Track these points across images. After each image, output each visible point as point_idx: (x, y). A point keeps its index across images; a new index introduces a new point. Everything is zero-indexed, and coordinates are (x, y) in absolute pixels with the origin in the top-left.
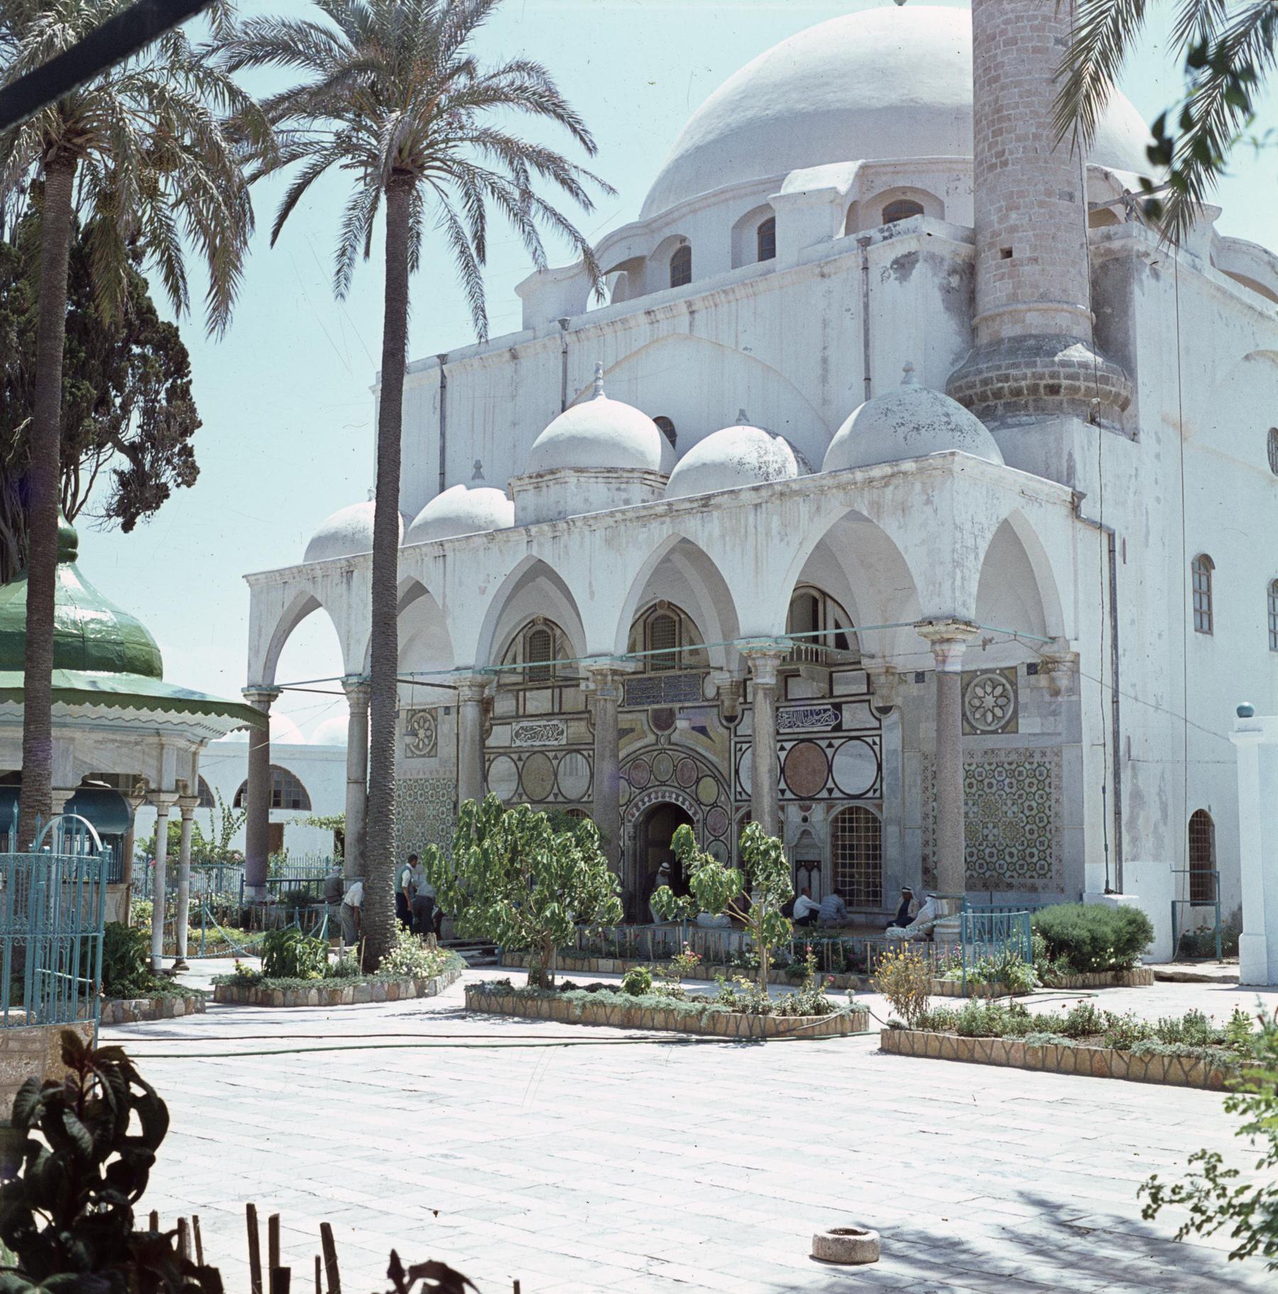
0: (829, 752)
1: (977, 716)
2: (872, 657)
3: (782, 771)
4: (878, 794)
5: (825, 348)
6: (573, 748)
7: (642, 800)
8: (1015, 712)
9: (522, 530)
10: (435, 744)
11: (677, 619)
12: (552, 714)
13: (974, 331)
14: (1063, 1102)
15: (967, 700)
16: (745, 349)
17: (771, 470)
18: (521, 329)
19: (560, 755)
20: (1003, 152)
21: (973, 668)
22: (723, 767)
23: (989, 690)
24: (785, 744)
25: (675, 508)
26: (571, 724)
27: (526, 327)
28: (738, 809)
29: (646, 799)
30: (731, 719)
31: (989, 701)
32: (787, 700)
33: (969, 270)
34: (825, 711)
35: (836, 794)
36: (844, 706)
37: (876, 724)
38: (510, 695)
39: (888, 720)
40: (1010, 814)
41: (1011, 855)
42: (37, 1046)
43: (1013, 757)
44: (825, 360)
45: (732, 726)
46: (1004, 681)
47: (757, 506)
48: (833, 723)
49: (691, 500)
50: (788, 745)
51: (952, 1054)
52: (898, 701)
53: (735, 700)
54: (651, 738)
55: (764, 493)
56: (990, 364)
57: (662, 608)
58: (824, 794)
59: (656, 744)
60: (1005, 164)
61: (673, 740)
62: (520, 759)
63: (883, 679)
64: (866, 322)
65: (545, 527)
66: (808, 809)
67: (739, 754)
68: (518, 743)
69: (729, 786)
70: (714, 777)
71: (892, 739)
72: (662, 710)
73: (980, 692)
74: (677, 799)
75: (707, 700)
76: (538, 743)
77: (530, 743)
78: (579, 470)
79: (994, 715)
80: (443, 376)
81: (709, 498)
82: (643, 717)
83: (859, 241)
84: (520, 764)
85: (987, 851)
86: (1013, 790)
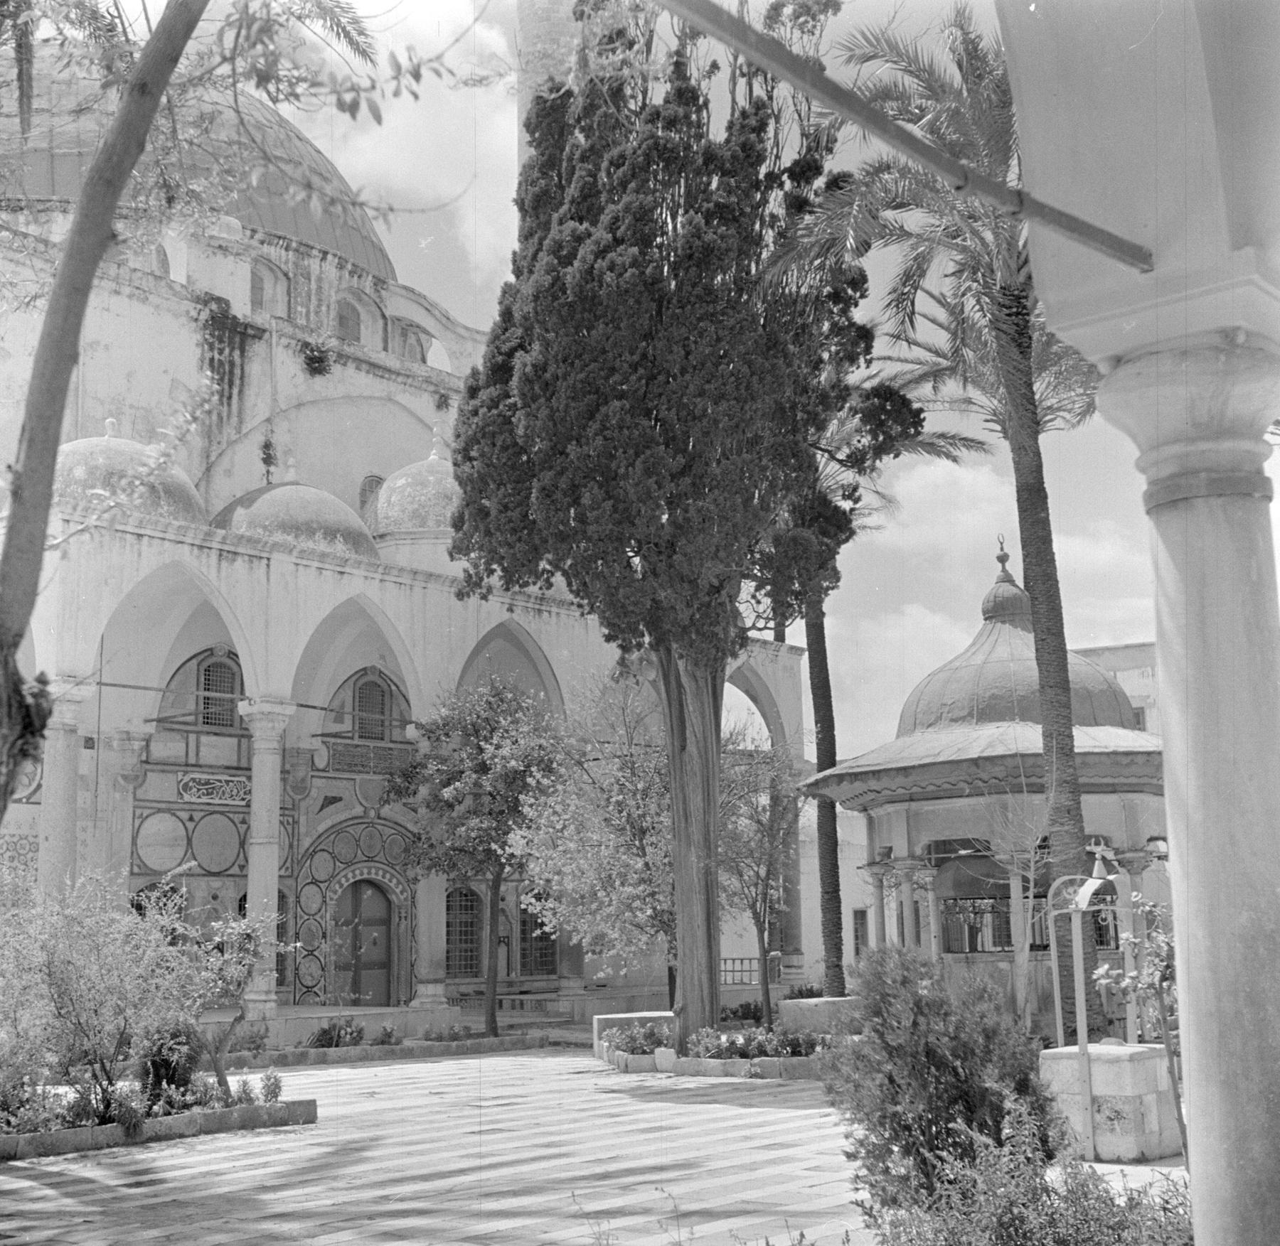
7: (345, 876)
10: (39, 786)
11: (386, 687)
29: (350, 875)
38: (178, 737)
57: (373, 673)
61: (383, 815)
62: (191, 819)
68: (187, 797)
74: (384, 877)
75: (318, 770)
76: (217, 801)
77: (205, 799)
82: (349, 784)
84: (190, 825)
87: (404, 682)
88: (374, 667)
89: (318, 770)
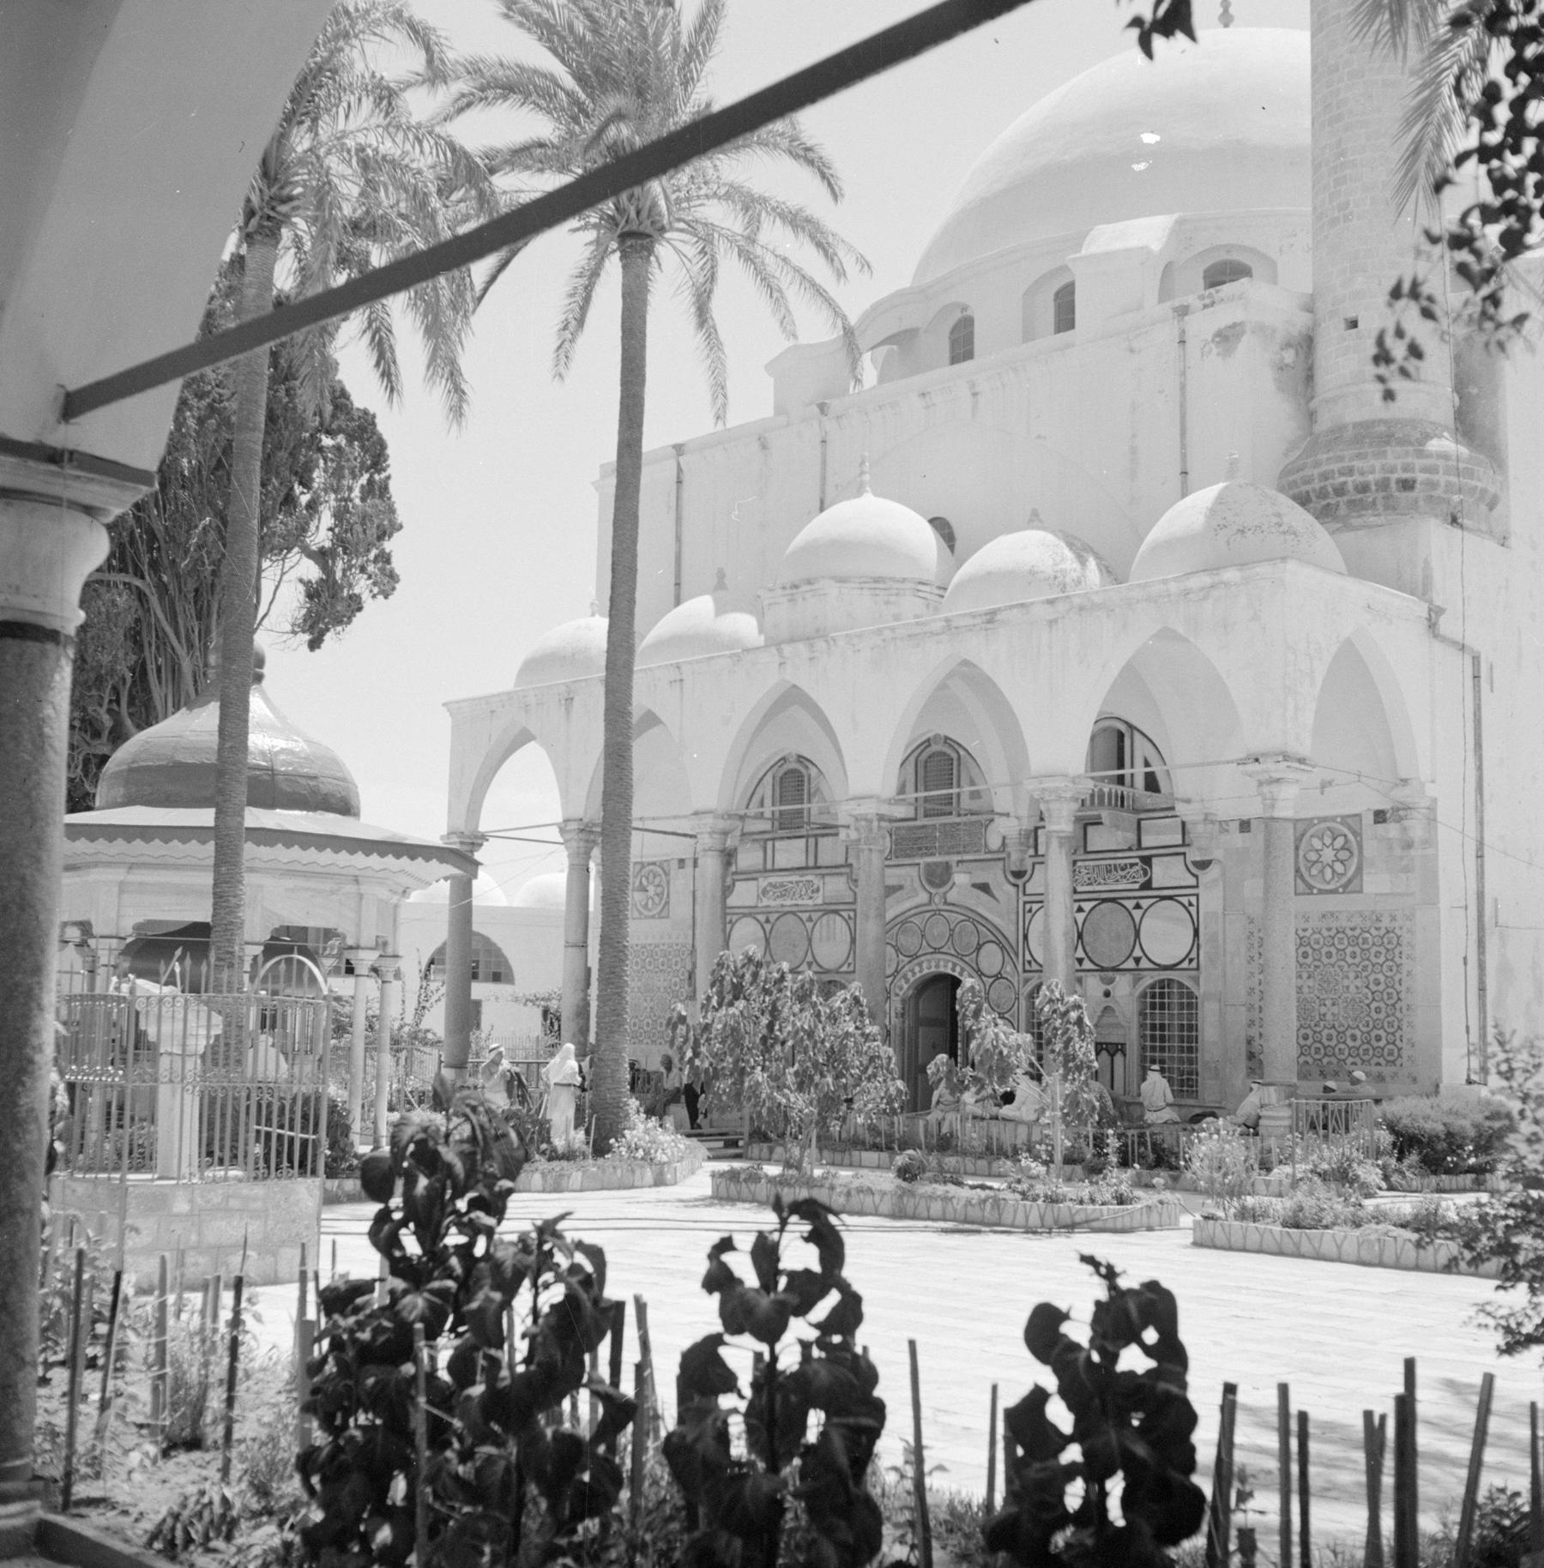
0: (1137, 914)
1: (1314, 872)
2: (1188, 801)
3: (1080, 936)
4: (1194, 965)
5: (1134, 436)
6: (830, 909)
7: (912, 971)
8: (1359, 869)
9: (773, 650)
10: (667, 903)
11: (954, 756)
12: (807, 868)
13: (1312, 416)
14: (1398, 1294)
15: (1301, 853)
16: (1039, 437)
17: (1068, 580)
18: (769, 412)
19: (815, 916)
20: (1348, 204)
21: (1310, 815)
22: (1009, 931)
23: (1328, 841)
24: (1083, 905)
25: (954, 624)
26: (827, 879)
27: (779, 410)
28: (1027, 981)
29: (917, 969)
30: (1018, 874)
31: (1328, 855)
32: (1086, 852)
33: (1307, 343)
34: (1132, 865)
35: (1144, 964)
36: (1154, 860)
37: (1192, 881)
38: (757, 845)
39: (1207, 876)
40: (1352, 988)
41: (1354, 1038)
42: (259, 1205)
43: (1357, 921)
44: (1134, 451)
45: (1020, 882)
46: (1346, 831)
47: (1052, 623)
48: (1142, 880)
49: (973, 616)
50: (1087, 906)
51: (1275, 1249)
52: (1217, 854)
53: (1025, 852)
54: (923, 897)
55: (1061, 607)
56: (1331, 454)
58: (1130, 964)
59: (930, 903)
60: (1346, 219)
62: (767, 921)
63: (1200, 828)
64: (1182, 406)
65: (801, 646)
66: (1111, 981)
67: (1028, 916)
68: (765, 902)
69: (1017, 954)
70: (999, 943)
71: (1210, 901)
72: (936, 864)
73: (1317, 843)
75: (990, 852)
76: (789, 902)
78: (842, 580)
79: (1334, 871)
80: (680, 470)
81: (993, 613)
82: (913, 871)
83: (1175, 310)
84: (768, 927)
85: (1326, 1032)
86: (1357, 960)
87: (763, 764)
88: (937, 736)
89: (990, 852)
